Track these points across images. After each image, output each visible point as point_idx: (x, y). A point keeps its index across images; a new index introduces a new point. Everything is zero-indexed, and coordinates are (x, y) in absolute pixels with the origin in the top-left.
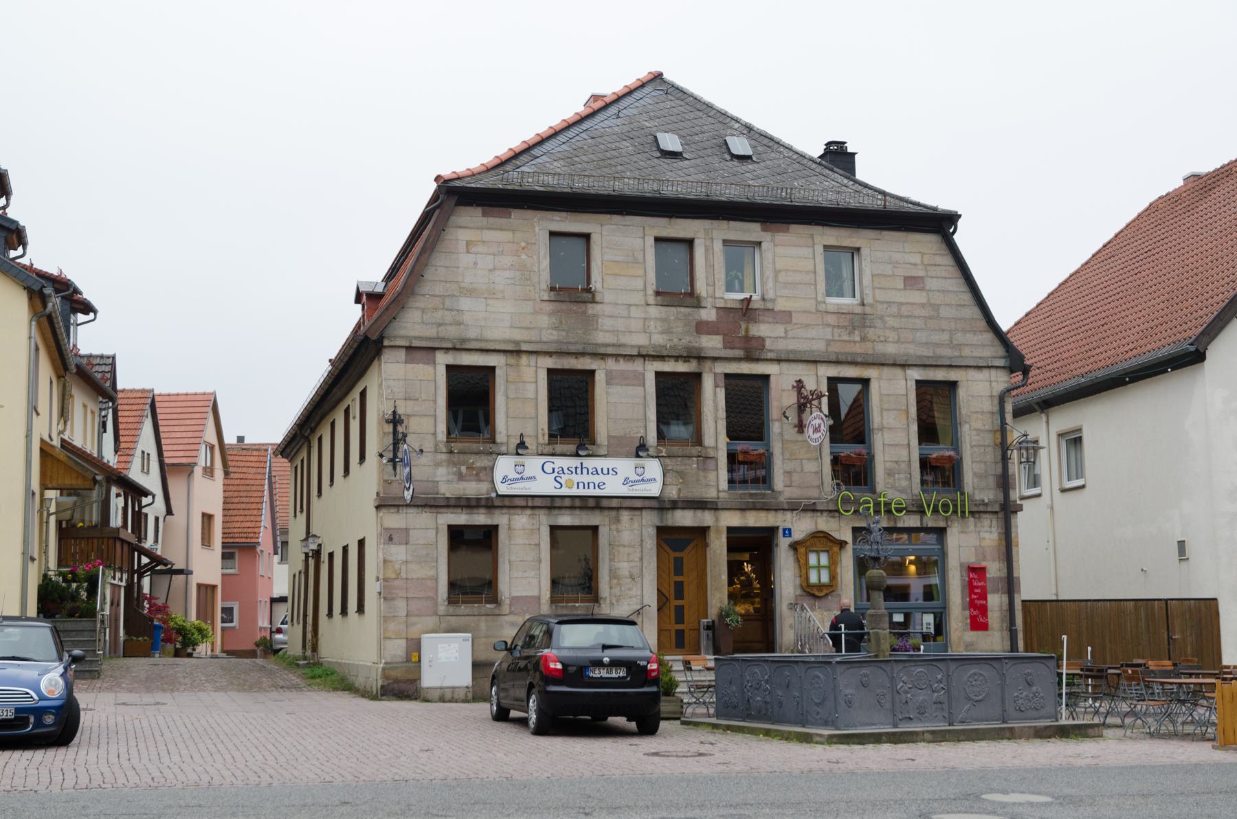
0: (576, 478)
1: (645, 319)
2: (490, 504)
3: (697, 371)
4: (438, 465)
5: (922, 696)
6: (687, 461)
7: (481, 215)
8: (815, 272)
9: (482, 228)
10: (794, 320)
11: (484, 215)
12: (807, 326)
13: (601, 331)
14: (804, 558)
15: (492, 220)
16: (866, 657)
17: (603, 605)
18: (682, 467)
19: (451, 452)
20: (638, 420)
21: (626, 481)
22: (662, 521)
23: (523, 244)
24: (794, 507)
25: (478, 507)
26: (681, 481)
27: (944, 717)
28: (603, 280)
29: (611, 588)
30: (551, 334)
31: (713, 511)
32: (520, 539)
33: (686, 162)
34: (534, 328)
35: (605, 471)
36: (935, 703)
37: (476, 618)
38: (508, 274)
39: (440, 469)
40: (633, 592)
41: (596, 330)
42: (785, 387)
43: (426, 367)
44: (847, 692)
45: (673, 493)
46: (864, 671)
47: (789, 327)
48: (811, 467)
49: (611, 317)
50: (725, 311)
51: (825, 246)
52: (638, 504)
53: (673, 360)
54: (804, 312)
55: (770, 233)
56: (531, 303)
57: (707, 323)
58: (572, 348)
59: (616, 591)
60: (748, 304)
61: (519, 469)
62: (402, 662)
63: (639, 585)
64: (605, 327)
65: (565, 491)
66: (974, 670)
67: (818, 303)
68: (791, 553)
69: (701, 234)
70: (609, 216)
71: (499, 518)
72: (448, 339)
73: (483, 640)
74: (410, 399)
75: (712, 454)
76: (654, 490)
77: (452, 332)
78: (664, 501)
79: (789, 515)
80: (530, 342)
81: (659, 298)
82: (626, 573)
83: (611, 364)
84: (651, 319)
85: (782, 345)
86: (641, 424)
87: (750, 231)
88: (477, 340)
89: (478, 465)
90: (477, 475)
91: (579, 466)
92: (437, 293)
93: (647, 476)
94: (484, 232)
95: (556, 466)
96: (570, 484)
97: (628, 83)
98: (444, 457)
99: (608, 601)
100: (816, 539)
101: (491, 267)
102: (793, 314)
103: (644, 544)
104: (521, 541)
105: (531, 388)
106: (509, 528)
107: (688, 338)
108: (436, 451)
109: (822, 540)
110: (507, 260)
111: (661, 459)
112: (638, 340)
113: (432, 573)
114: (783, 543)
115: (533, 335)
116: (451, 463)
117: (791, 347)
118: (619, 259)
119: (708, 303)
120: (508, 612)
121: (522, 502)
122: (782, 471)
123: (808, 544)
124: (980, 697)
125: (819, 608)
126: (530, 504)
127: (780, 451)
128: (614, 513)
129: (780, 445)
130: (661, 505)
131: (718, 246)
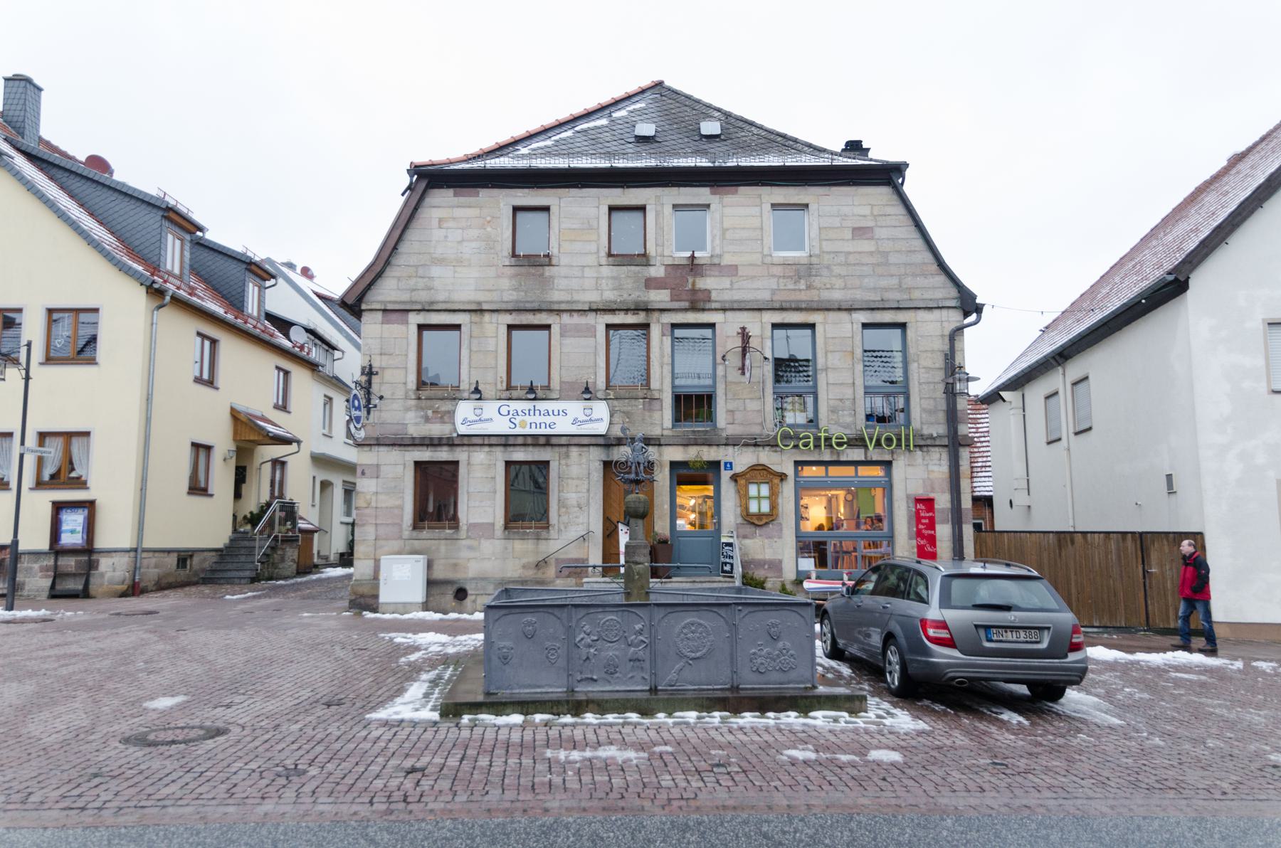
0: (529, 419)
1: (597, 278)
2: (451, 443)
3: (645, 322)
4: (407, 409)
5: (611, 652)
6: (633, 402)
7: (452, 195)
8: (762, 229)
9: (453, 207)
10: (740, 273)
11: (455, 195)
12: (753, 277)
13: (557, 290)
14: (744, 489)
15: (462, 200)
16: (721, 590)
17: (552, 532)
18: (630, 408)
19: (419, 398)
20: (589, 367)
21: (575, 422)
22: (608, 456)
23: (489, 218)
24: (732, 442)
25: (440, 445)
26: (627, 420)
27: (643, 678)
28: (559, 245)
29: (560, 516)
30: (511, 295)
31: (656, 447)
32: (478, 473)
33: (657, 144)
34: (495, 290)
35: (556, 413)
36: (630, 660)
37: (436, 542)
38: (474, 245)
39: (409, 413)
40: (580, 520)
41: (552, 289)
42: (729, 334)
43: (400, 326)
44: (502, 644)
45: (617, 432)
46: (529, 618)
47: (735, 279)
48: (753, 405)
49: (565, 277)
50: (673, 267)
51: (773, 205)
52: (585, 441)
53: (622, 313)
54: (751, 265)
55: (718, 196)
56: (494, 268)
57: (656, 279)
58: (529, 306)
59: (564, 518)
60: (693, 261)
61: (478, 412)
62: (370, 580)
63: (586, 514)
64: (560, 287)
65: (518, 431)
66: (690, 618)
67: (764, 256)
68: (733, 484)
69: (652, 201)
70: (567, 190)
71: (460, 455)
72: (420, 303)
73: (442, 561)
74: (385, 354)
75: (657, 396)
76: (601, 428)
77: (423, 296)
78: (610, 438)
79: (730, 449)
80: (492, 302)
81: (610, 259)
82: (575, 503)
83: (566, 318)
84: (603, 278)
85: (727, 296)
86: (591, 370)
87: (701, 194)
88: (445, 302)
89: (443, 409)
90: (442, 417)
91: (532, 408)
92: (412, 264)
93: (594, 416)
94: (455, 210)
95: (511, 409)
96: (523, 424)
97: (628, 91)
98: (413, 402)
99: (556, 527)
100: (755, 472)
101: (460, 239)
102: (740, 268)
103: (591, 477)
104: (479, 475)
105: (492, 342)
106: (469, 464)
107: (637, 294)
108: (406, 398)
109: (760, 472)
110: (474, 233)
111: (610, 401)
112: (592, 297)
113: (398, 503)
114: (725, 475)
115: (494, 296)
116: (419, 408)
117: (736, 298)
118: (574, 226)
119: (658, 261)
120: (464, 537)
121: (479, 441)
122: (725, 410)
123: (748, 476)
124: (698, 654)
125: (760, 535)
126: (486, 442)
127: (724, 391)
128: (564, 449)
129: (724, 386)
130: (607, 442)
131: (668, 210)
